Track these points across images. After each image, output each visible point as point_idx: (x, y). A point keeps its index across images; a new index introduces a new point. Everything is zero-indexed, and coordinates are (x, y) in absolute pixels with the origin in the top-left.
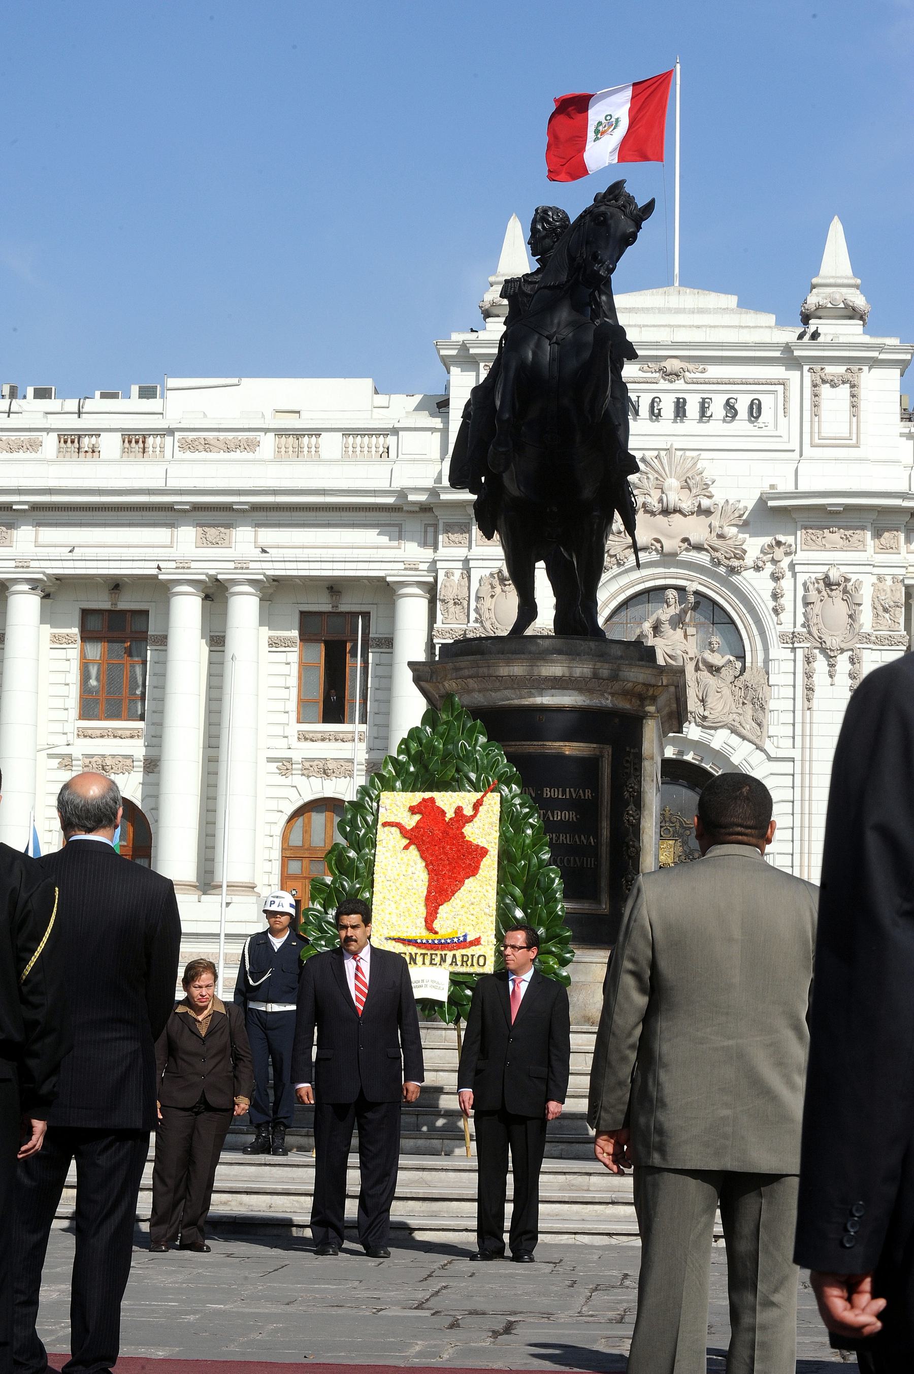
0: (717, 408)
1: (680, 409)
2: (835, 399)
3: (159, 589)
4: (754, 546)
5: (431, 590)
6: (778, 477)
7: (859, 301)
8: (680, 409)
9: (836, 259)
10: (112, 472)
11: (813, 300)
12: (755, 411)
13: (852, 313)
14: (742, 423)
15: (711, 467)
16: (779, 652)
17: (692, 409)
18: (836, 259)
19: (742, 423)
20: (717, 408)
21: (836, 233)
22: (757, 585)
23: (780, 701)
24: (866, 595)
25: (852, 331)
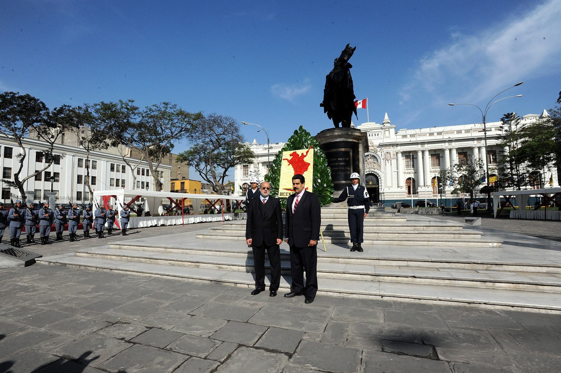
0: (374, 135)
2: (387, 133)
4: (379, 149)
6: (381, 141)
7: (389, 121)
9: (386, 117)
12: (378, 135)
13: (389, 123)
14: (376, 136)
18: (386, 117)
19: (376, 136)
20: (374, 135)
21: (386, 114)
22: (379, 153)
23: (382, 166)
24: (392, 154)
25: (389, 125)
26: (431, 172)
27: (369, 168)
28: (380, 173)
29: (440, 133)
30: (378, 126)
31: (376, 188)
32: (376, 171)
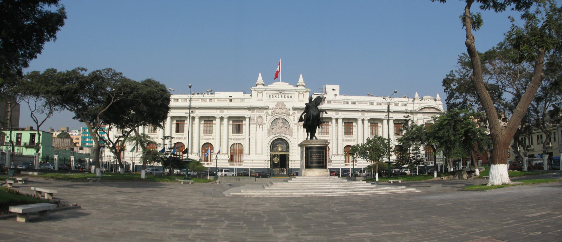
0: (286, 97)
1: (282, 97)
2: (301, 96)
3: (214, 118)
5: (250, 118)
7: (304, 84)
8: (282, 97)
10: (208, 104)
11: (298, 84)
12: (291, 97)
15: (285, 104)
16: (294, 125)
17: (283, 97)
20: (286, 97)
21: (301, 76)
25: (303, 88)
26: (343, 140)
27: (280, 133)
28: (291, 139)
29: (354, 103)
30: (292, 87)
31: (285, 156)
32: (286, 136)
